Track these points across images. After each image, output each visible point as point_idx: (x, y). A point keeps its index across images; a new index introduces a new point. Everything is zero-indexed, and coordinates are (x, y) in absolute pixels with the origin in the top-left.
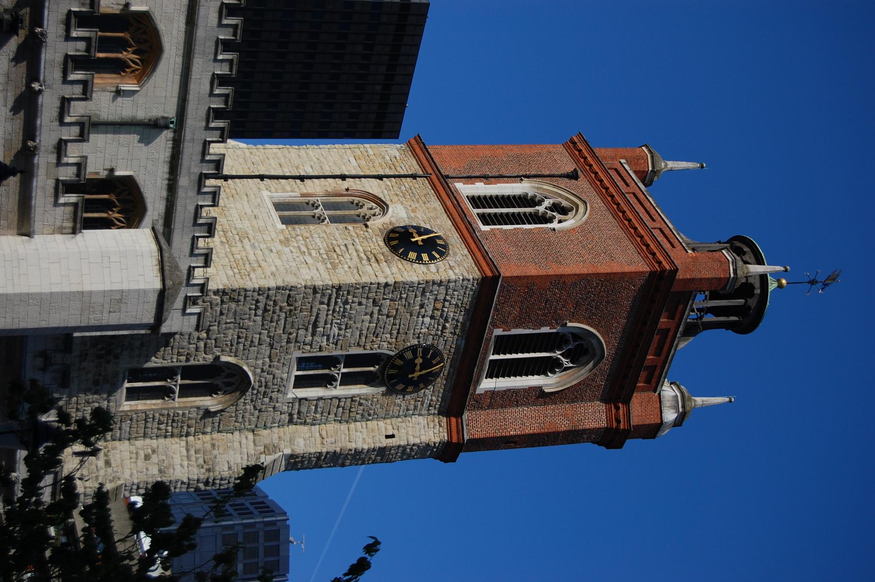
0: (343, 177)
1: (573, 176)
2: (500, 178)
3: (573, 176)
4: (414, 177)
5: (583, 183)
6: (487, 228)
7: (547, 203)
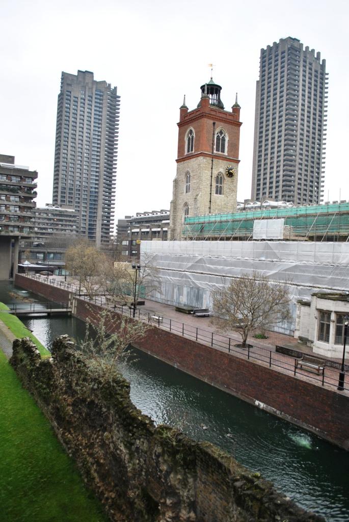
0: (212, 176)
1: (214, 124)
2: (213, 141)
3: (214, 124)
4: (212, 161)
5: (217, 123)
6: (226, 154)
7: (219, 134)
